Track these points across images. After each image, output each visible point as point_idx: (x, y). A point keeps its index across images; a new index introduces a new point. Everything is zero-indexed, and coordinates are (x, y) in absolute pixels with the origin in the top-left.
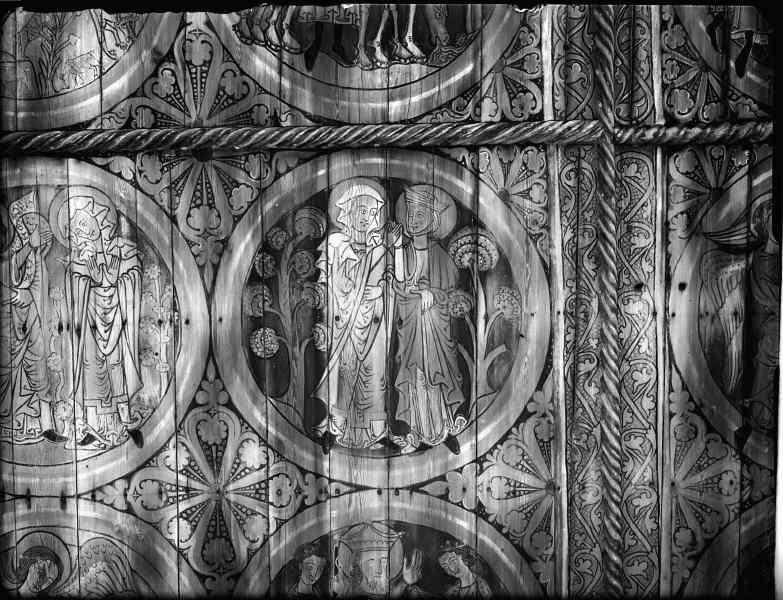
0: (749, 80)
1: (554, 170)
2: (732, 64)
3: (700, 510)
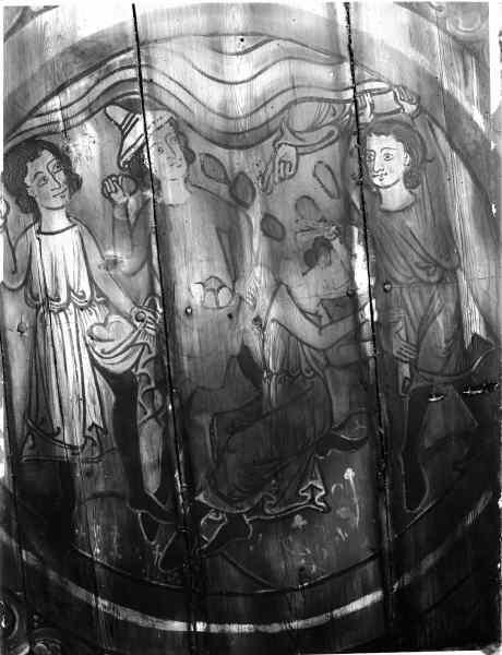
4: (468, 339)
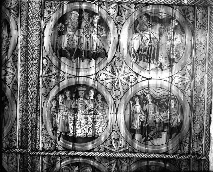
0: (61, 142)
1: (19, 158)
2: (57, 138)
4: (178, 122)
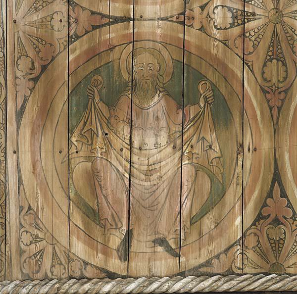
3: (37, 43)
